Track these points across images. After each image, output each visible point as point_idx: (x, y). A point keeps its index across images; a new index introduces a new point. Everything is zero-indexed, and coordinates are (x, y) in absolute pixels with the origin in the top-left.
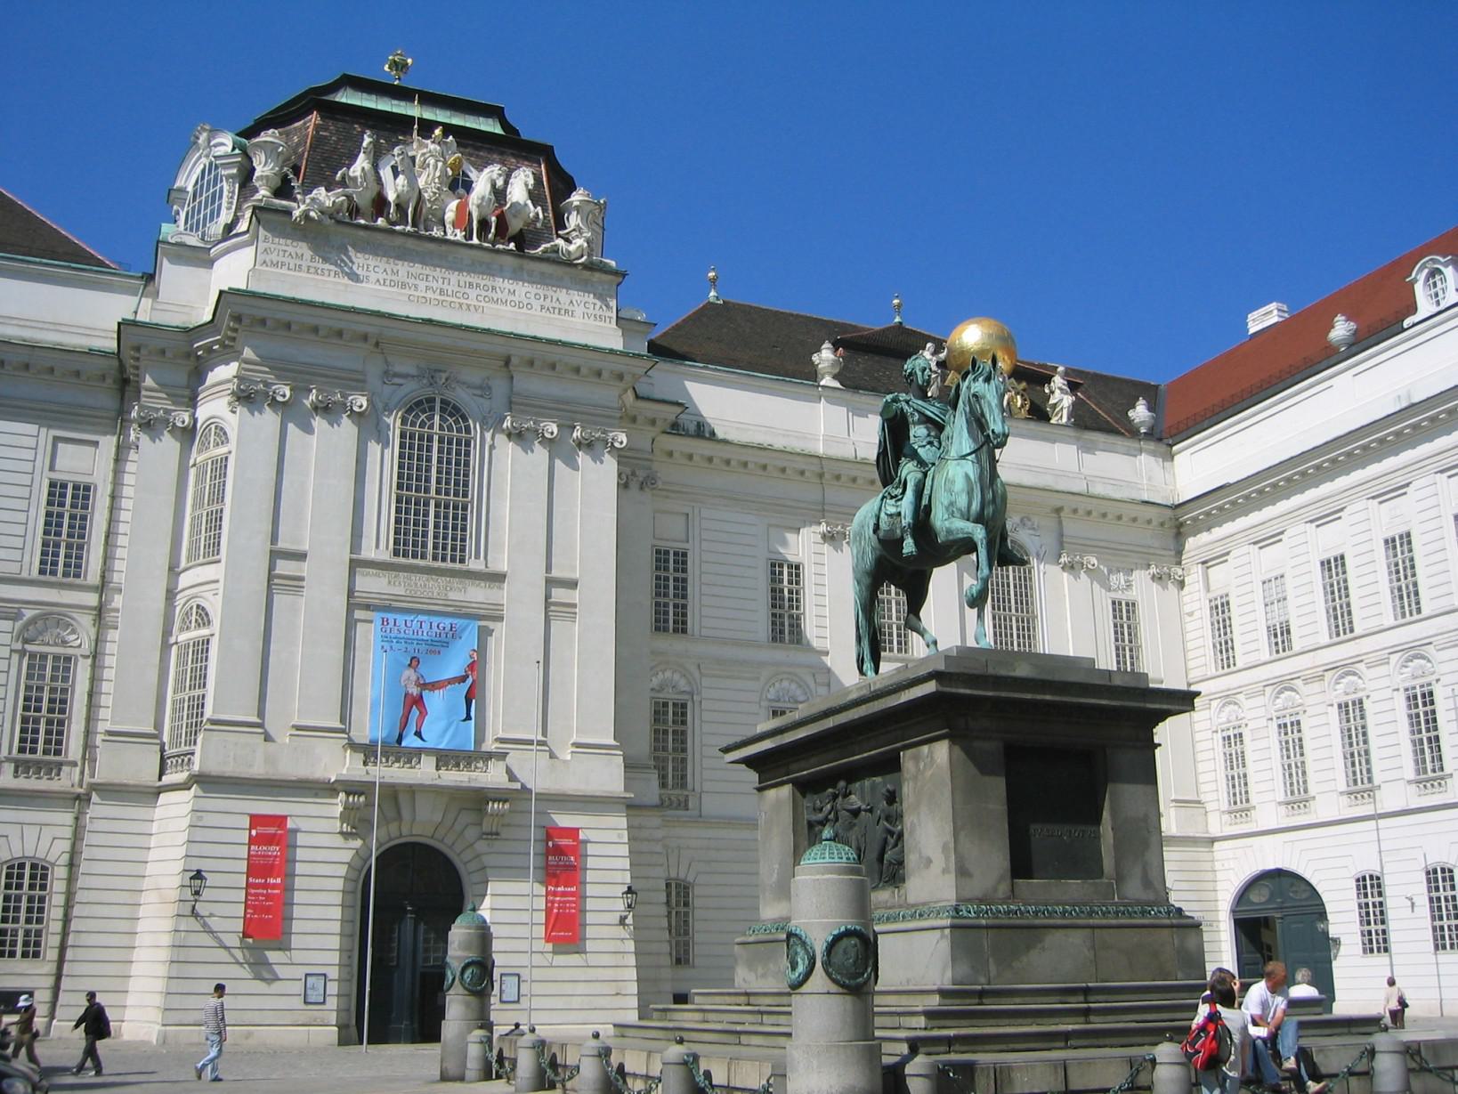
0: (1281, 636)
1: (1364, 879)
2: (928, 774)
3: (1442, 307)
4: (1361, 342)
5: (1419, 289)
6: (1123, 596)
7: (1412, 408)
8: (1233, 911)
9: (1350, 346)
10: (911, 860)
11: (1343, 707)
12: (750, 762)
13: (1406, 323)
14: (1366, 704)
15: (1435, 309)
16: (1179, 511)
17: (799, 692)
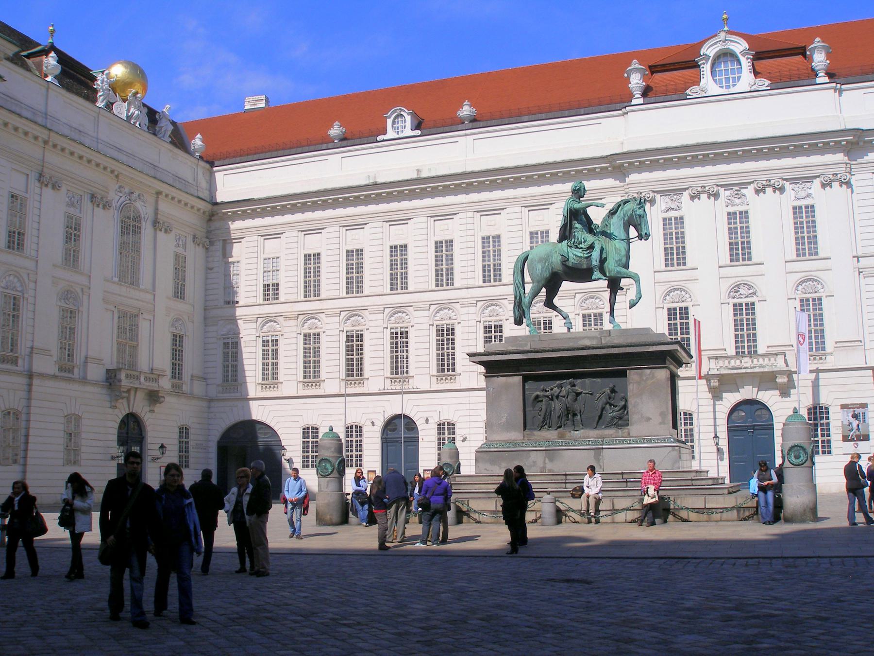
0: (271, 291)
1: (308, 428)
2: (649, 382)
3: (401, 135)
4: (346, 140)
5: (389, 122)
6: (180, 250)
7: (376, 185)
8: (219, 442)
9: (341, 140)
10: (633, 417)
11: (306, 336)
12: (481, 363)
13: (379, 138)
14: (322, 336)
15: (397, 136)
16: (216, 208)
17: (18, 285)
